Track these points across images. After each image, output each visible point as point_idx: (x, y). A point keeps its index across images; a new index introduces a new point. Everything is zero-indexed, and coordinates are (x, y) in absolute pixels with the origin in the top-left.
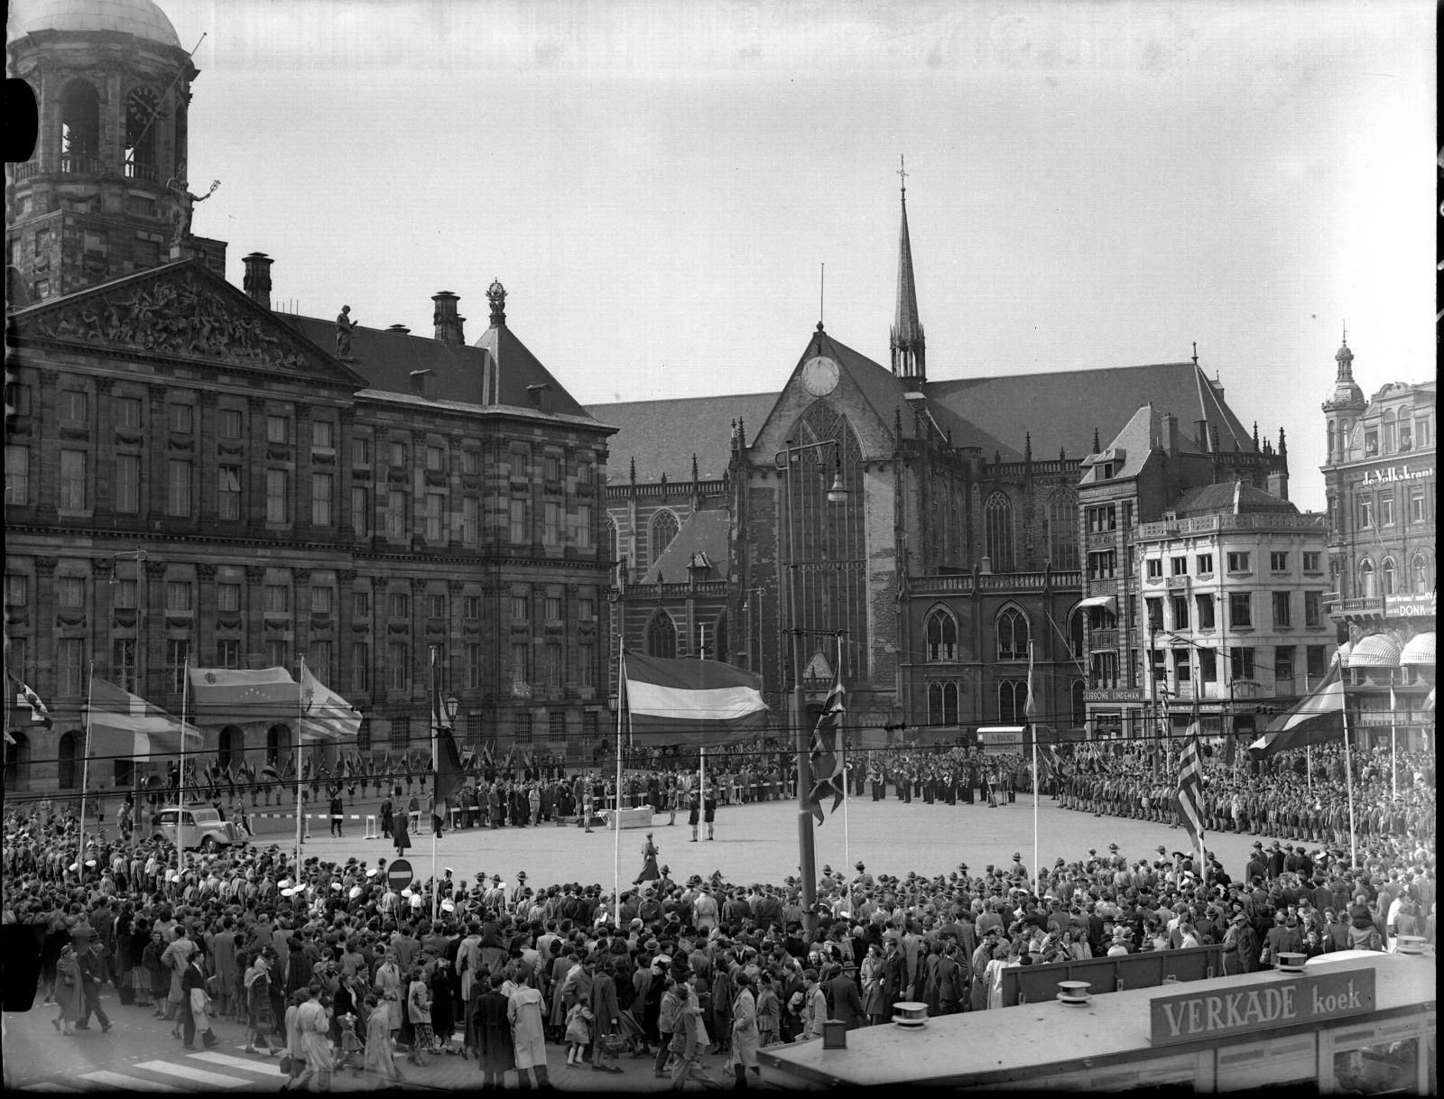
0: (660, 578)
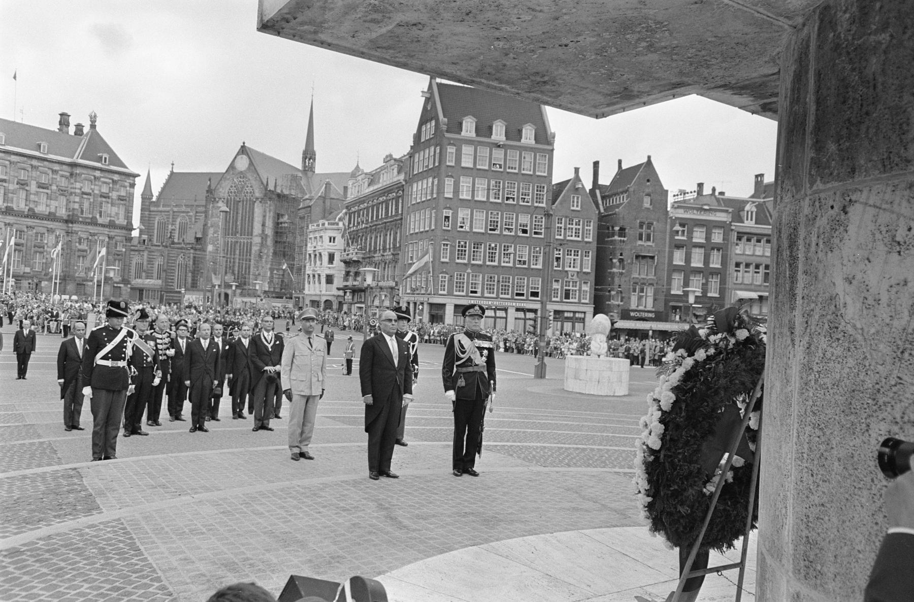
0: (183, 241)
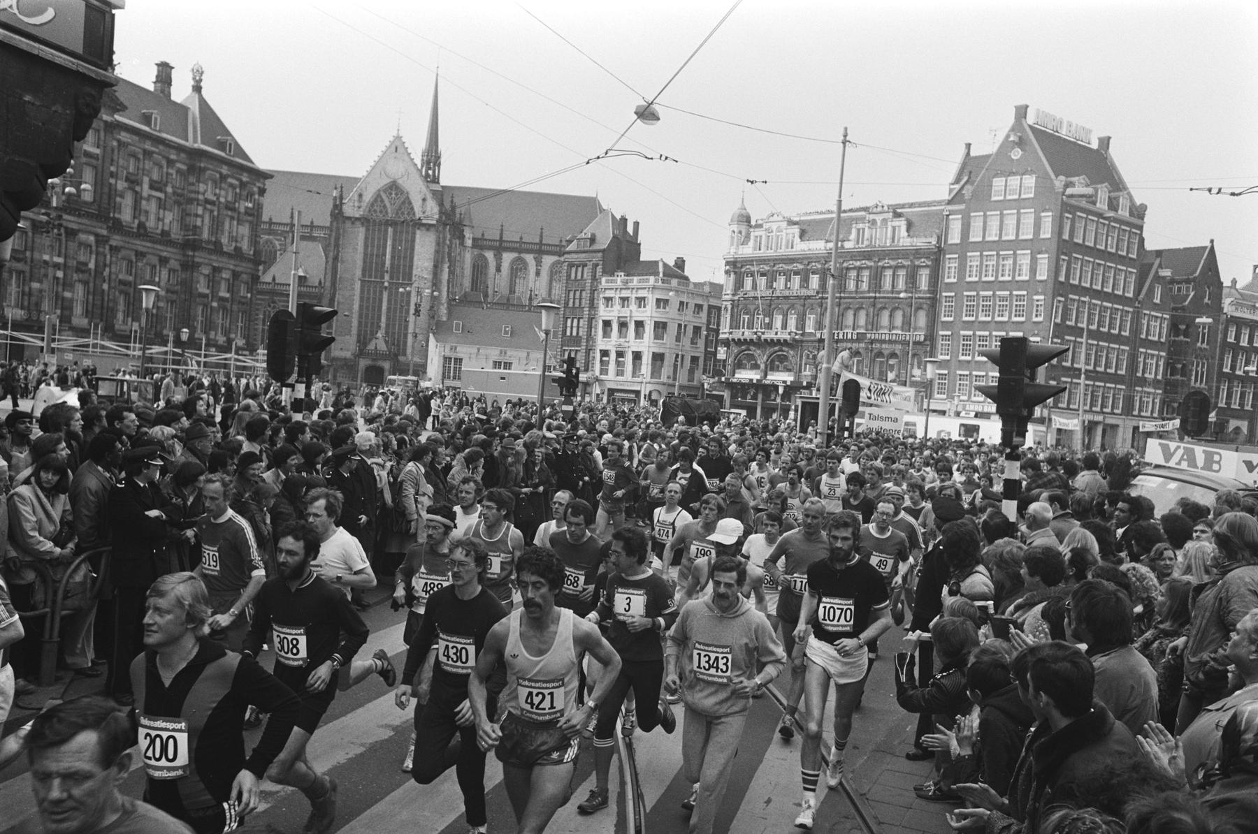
0: (274, 279)
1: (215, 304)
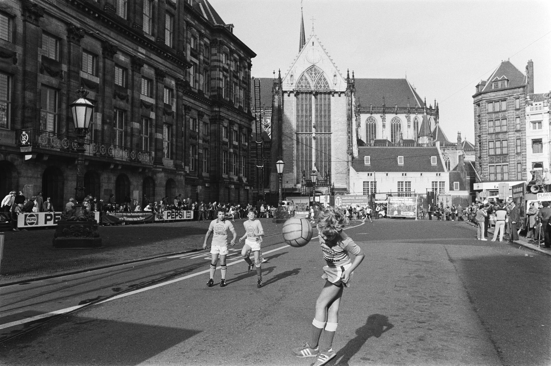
1: (232, 150)
